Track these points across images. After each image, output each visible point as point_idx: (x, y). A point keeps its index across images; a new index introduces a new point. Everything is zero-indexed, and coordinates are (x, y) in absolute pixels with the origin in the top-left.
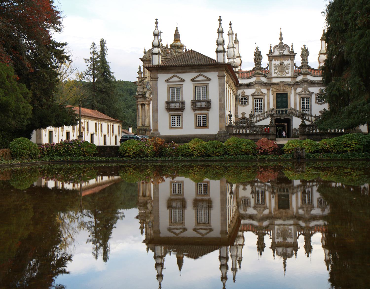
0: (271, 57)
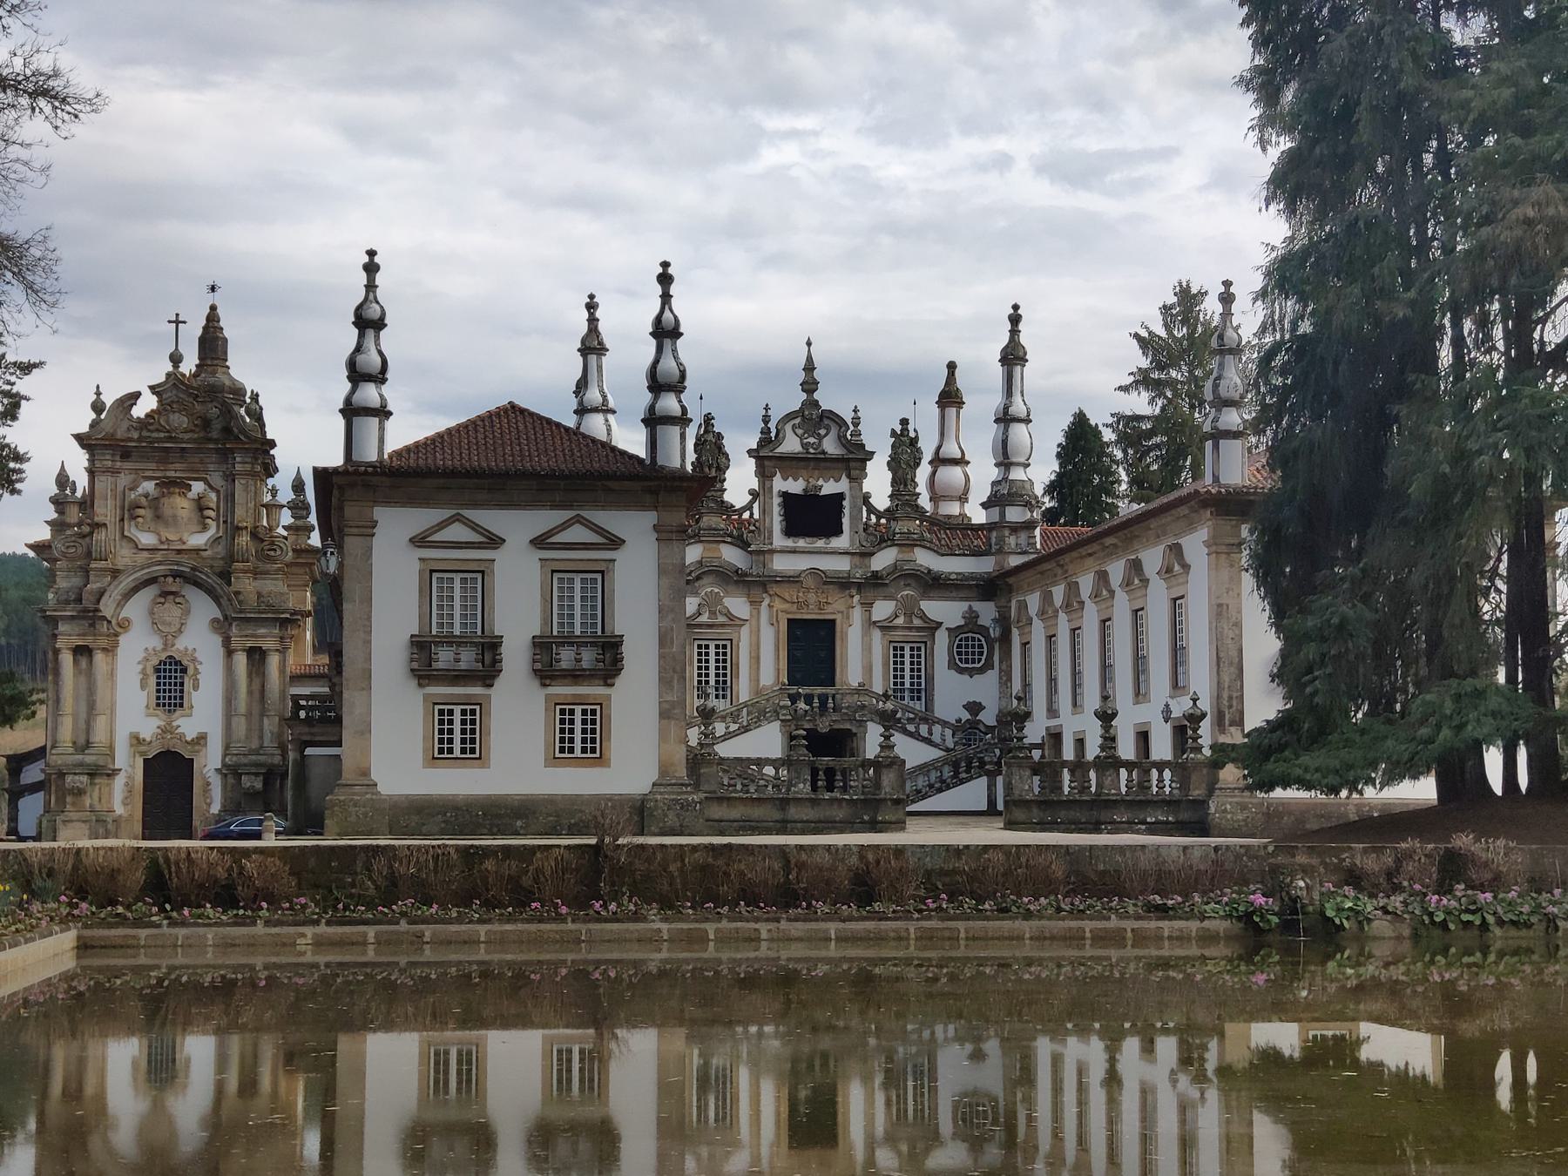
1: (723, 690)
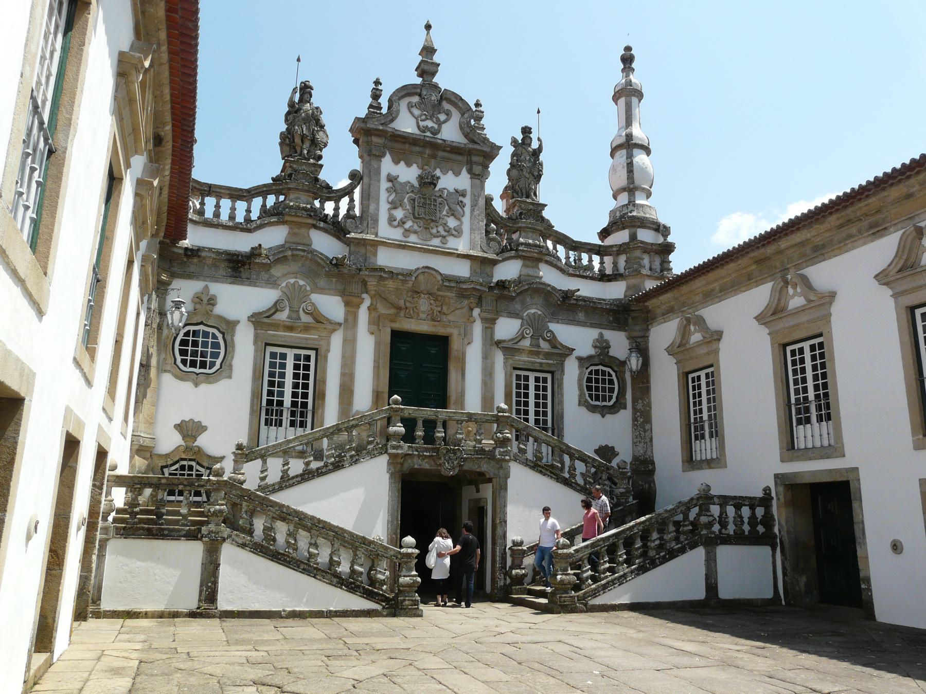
0: (375, 139)
1: (303, 415)
